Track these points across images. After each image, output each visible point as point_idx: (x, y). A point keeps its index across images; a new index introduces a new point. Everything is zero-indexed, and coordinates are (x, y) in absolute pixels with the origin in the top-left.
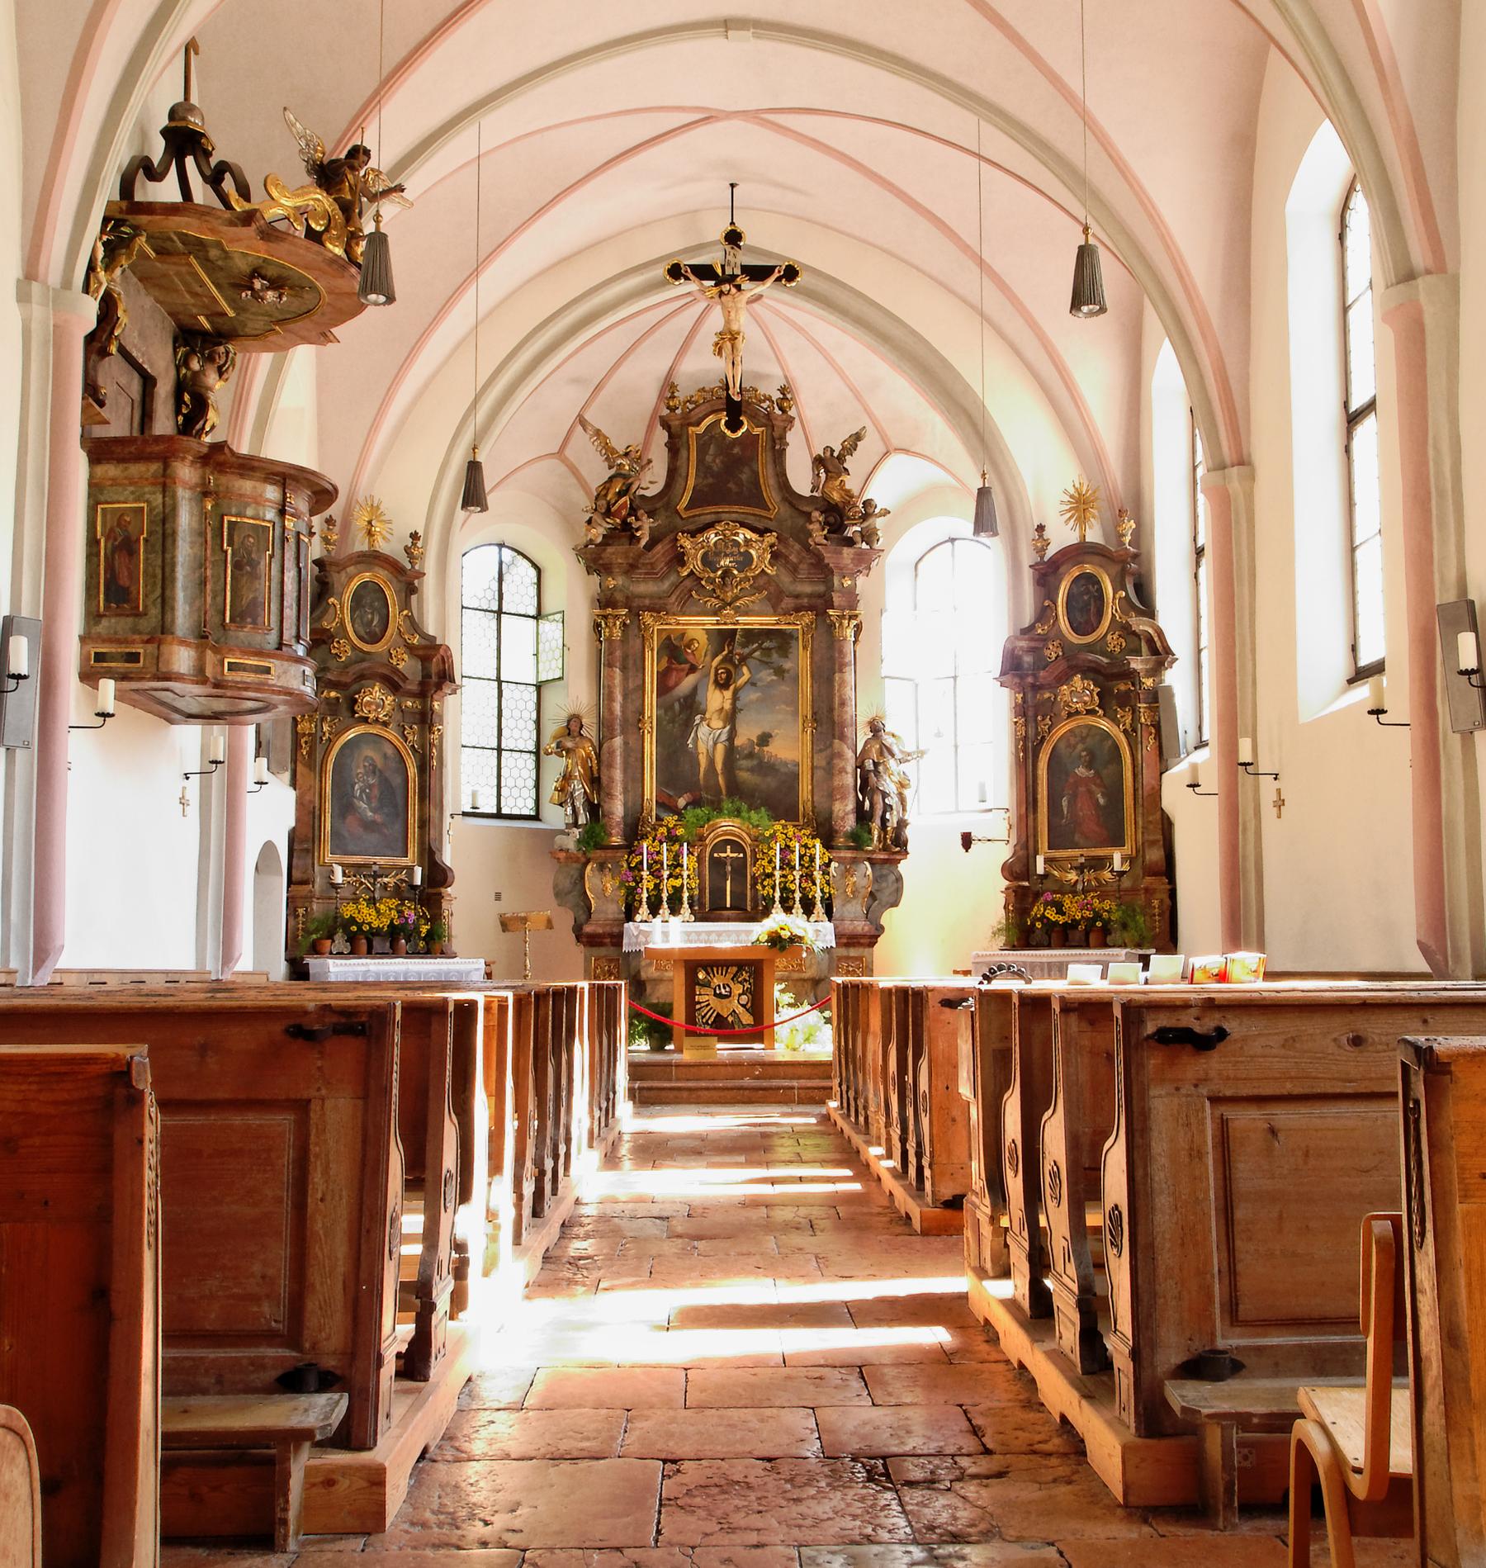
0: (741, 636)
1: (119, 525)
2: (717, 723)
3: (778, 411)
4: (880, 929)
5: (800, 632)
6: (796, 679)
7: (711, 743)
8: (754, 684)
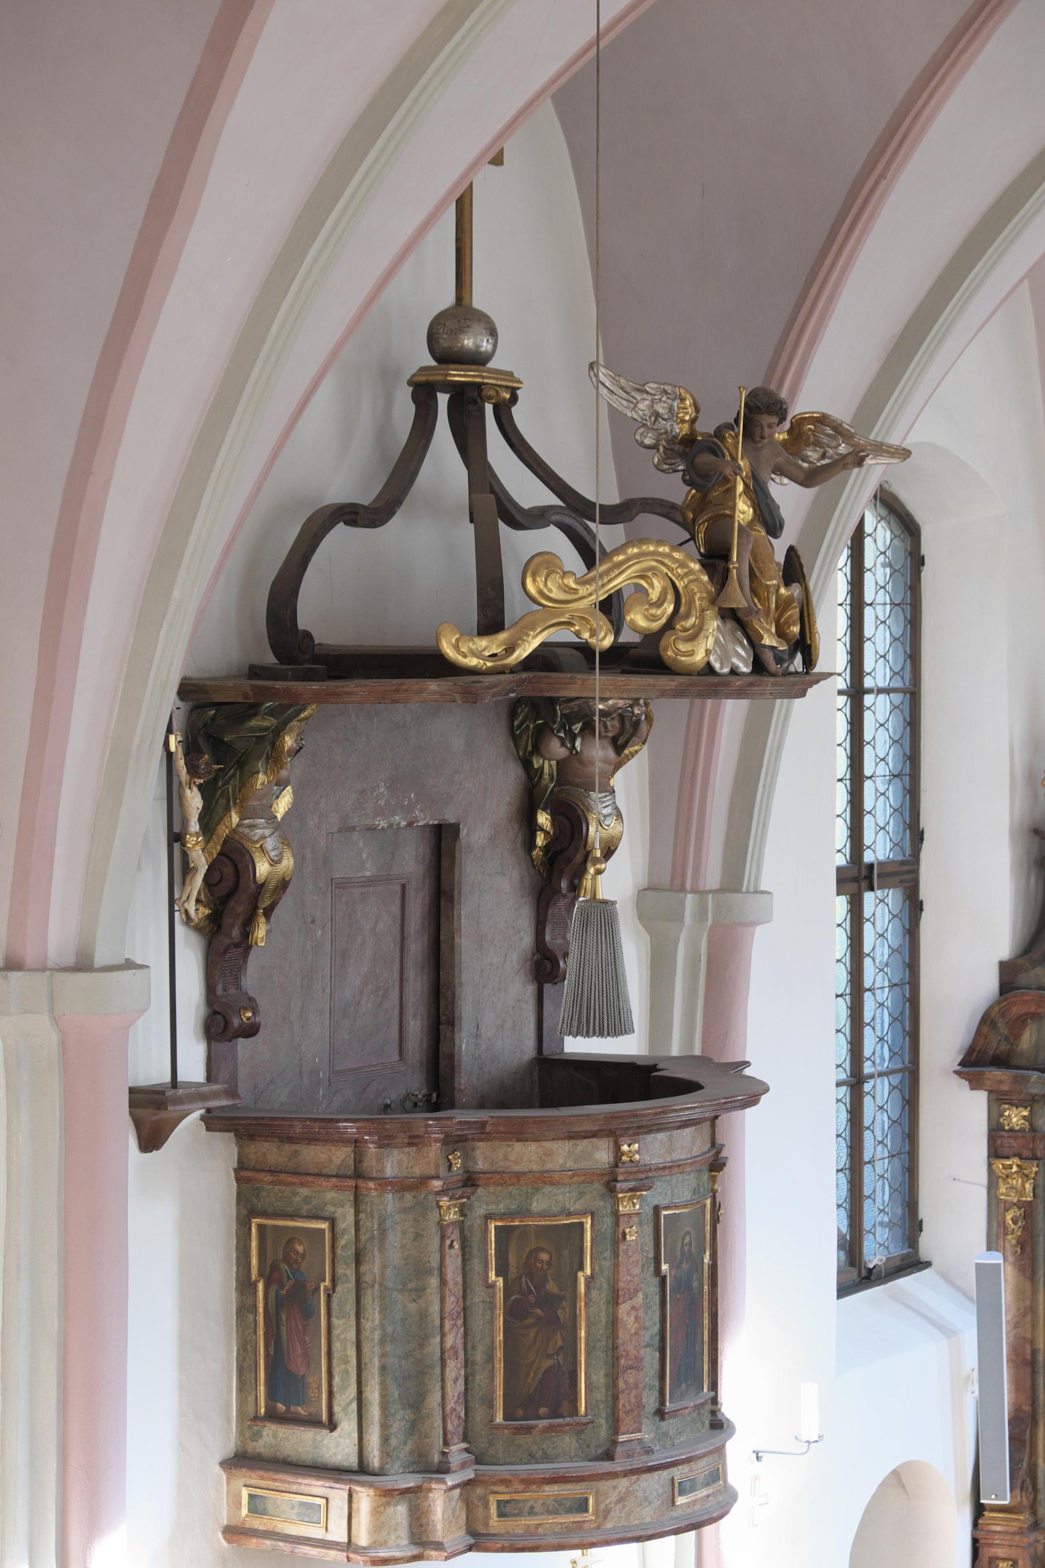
1: (286, 1259)
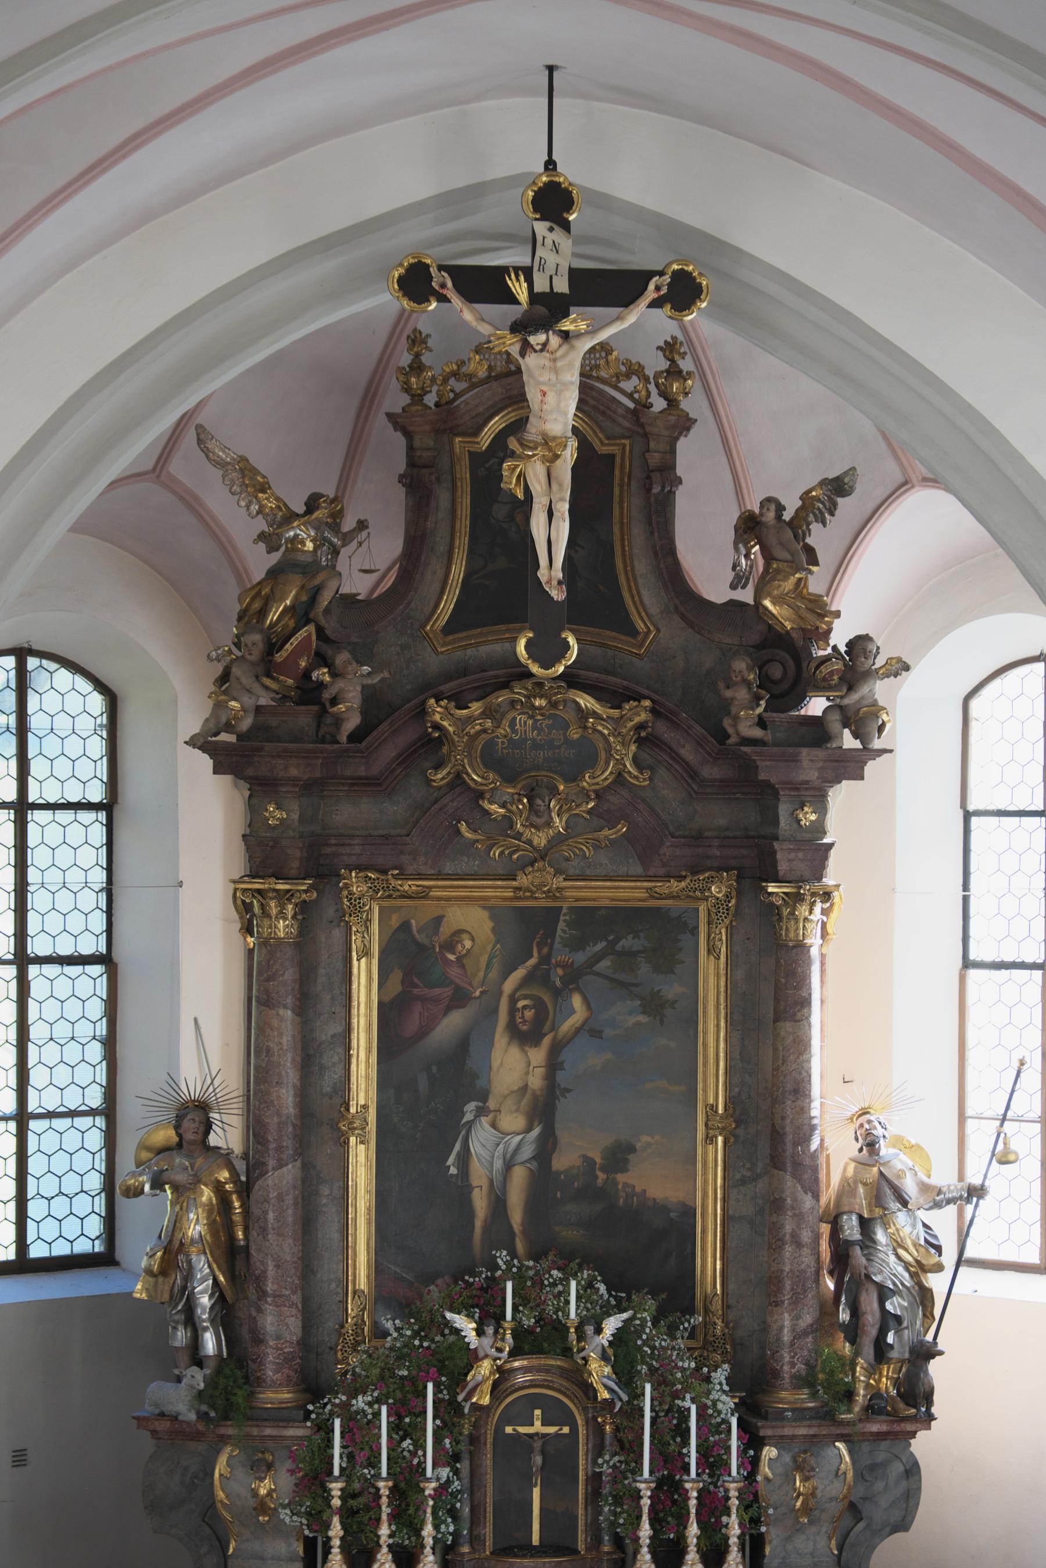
0: (568, 924)
2: (513, 1121)
3: (659, 404)
6: (691, 1021)
7: (498, 1164)
8: (596, 1033)
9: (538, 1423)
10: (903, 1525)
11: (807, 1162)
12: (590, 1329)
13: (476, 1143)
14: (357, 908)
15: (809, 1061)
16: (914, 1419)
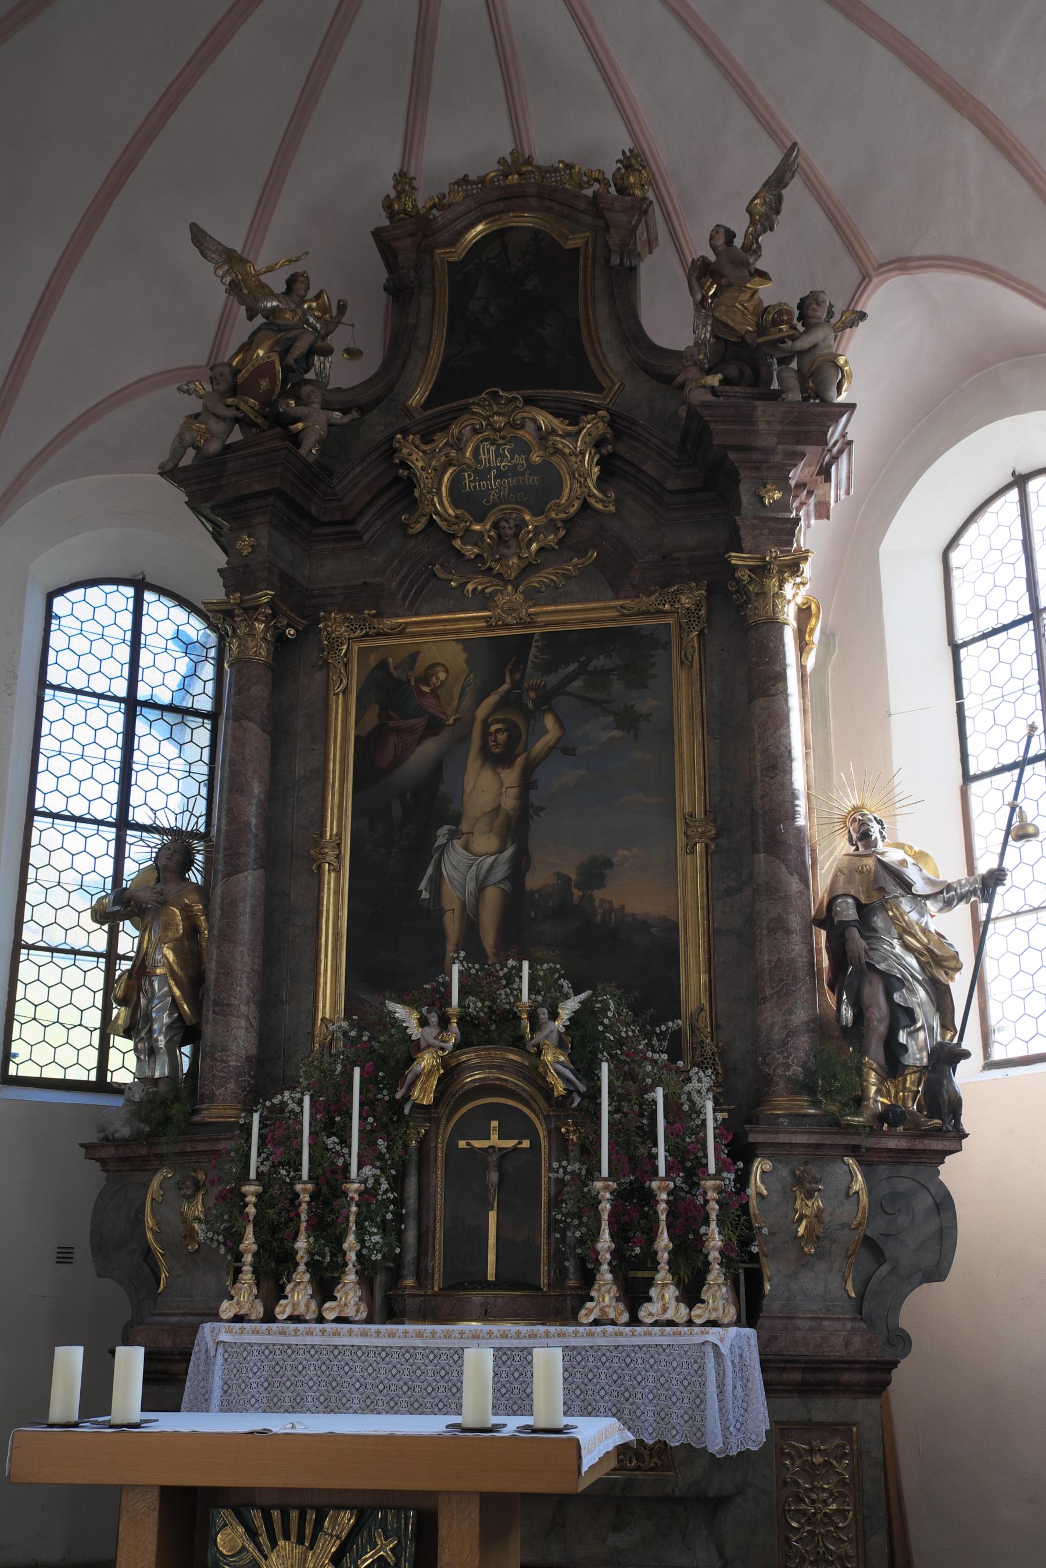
2: (485, 842)
4: (902, 1341)
5: (674, 631)
6: (667, 734)
7: (471, 886)
8: (569, 751)
9: (494, 1136)
10: (937, 1272)
11: (792, 841)
12: (543, 1013)
13: (448, 866)
14: (335, 644)
15: (788, 736)
16: (938, 1133)
